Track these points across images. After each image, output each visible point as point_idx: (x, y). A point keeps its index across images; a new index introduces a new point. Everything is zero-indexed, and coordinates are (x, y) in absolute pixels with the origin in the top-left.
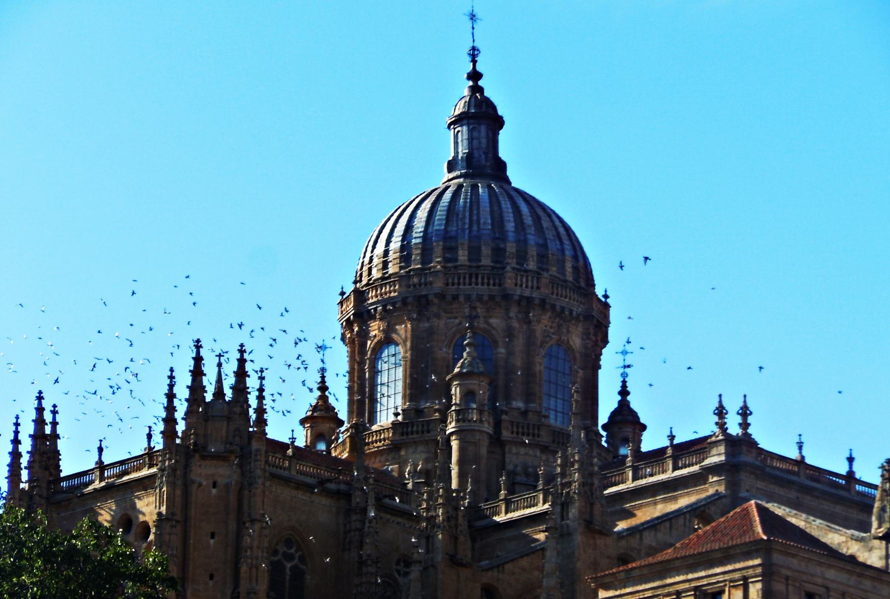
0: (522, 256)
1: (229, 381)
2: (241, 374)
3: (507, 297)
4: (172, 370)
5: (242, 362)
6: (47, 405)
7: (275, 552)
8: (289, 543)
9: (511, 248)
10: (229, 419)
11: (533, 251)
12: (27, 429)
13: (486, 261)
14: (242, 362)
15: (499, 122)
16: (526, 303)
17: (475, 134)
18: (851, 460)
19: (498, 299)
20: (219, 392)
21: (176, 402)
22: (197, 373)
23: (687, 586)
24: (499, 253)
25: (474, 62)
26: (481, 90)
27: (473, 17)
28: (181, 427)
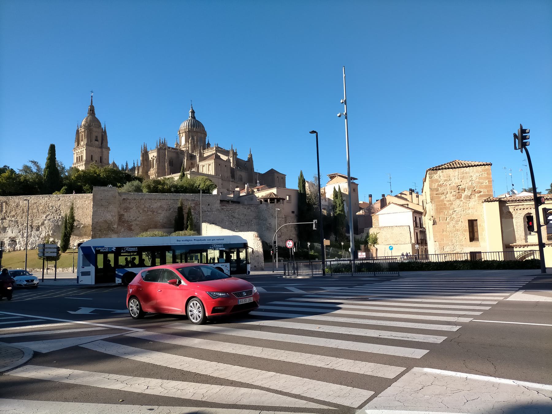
1: (163, 142)
2: (165, 141)
5: (165, 139)
6: (145, 144)
8: (171, 158)
12: (143, 146)
14: (165, 139)
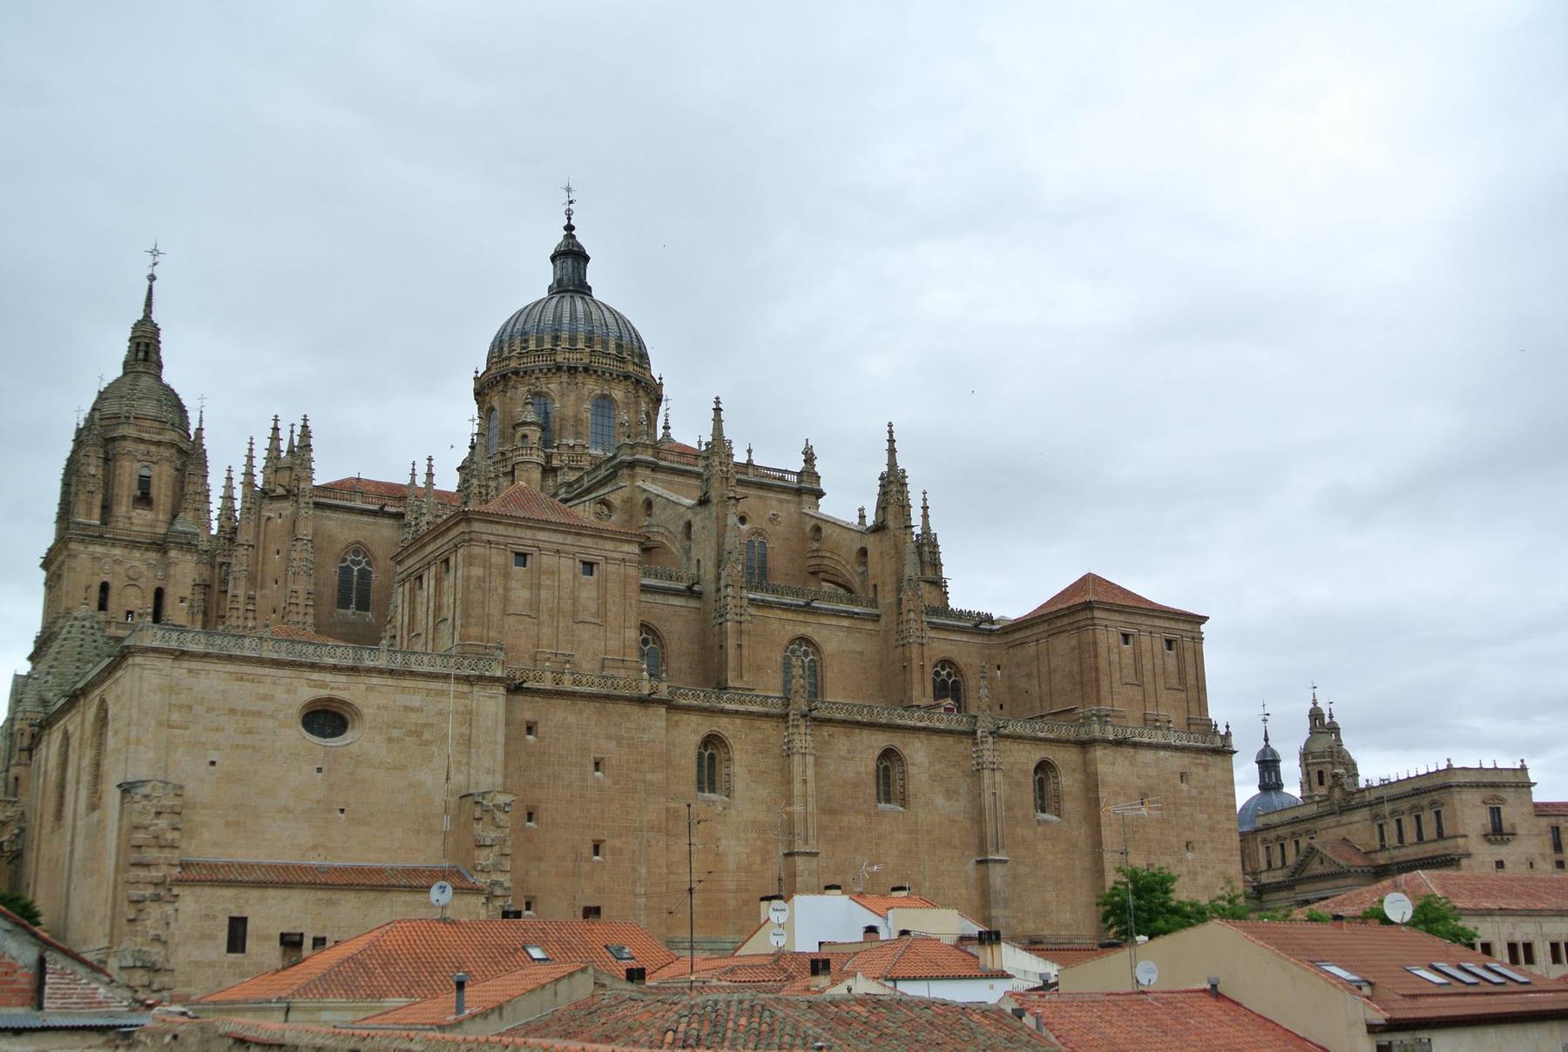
0: (573, 340)
3: (559, 368)
4: (251, 439)
7: (344, 560)
8: (357, 553)
9: (565, 335)
10: (291, 469)
11: (581, 336)
13: (548, 346)
15: (587, 259)
16: (573, 370)
17: (564, 265)
18: (749, 451)
19: (554, 371)
20: (291, 451)
21: (255, 462)
22: (275, 438)
23: (432, 556)
24: (556, 338)
25: (569, 219)
26: (574, 237)
27: (569, 190)
28: (259, 481)
